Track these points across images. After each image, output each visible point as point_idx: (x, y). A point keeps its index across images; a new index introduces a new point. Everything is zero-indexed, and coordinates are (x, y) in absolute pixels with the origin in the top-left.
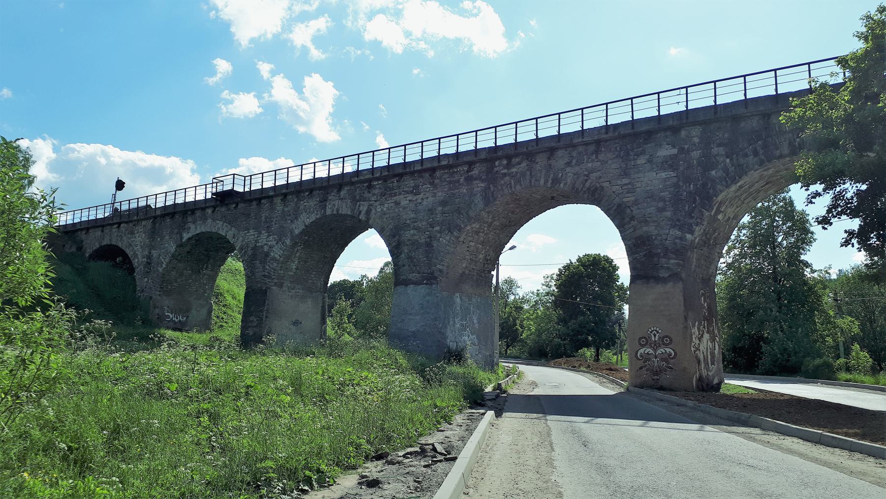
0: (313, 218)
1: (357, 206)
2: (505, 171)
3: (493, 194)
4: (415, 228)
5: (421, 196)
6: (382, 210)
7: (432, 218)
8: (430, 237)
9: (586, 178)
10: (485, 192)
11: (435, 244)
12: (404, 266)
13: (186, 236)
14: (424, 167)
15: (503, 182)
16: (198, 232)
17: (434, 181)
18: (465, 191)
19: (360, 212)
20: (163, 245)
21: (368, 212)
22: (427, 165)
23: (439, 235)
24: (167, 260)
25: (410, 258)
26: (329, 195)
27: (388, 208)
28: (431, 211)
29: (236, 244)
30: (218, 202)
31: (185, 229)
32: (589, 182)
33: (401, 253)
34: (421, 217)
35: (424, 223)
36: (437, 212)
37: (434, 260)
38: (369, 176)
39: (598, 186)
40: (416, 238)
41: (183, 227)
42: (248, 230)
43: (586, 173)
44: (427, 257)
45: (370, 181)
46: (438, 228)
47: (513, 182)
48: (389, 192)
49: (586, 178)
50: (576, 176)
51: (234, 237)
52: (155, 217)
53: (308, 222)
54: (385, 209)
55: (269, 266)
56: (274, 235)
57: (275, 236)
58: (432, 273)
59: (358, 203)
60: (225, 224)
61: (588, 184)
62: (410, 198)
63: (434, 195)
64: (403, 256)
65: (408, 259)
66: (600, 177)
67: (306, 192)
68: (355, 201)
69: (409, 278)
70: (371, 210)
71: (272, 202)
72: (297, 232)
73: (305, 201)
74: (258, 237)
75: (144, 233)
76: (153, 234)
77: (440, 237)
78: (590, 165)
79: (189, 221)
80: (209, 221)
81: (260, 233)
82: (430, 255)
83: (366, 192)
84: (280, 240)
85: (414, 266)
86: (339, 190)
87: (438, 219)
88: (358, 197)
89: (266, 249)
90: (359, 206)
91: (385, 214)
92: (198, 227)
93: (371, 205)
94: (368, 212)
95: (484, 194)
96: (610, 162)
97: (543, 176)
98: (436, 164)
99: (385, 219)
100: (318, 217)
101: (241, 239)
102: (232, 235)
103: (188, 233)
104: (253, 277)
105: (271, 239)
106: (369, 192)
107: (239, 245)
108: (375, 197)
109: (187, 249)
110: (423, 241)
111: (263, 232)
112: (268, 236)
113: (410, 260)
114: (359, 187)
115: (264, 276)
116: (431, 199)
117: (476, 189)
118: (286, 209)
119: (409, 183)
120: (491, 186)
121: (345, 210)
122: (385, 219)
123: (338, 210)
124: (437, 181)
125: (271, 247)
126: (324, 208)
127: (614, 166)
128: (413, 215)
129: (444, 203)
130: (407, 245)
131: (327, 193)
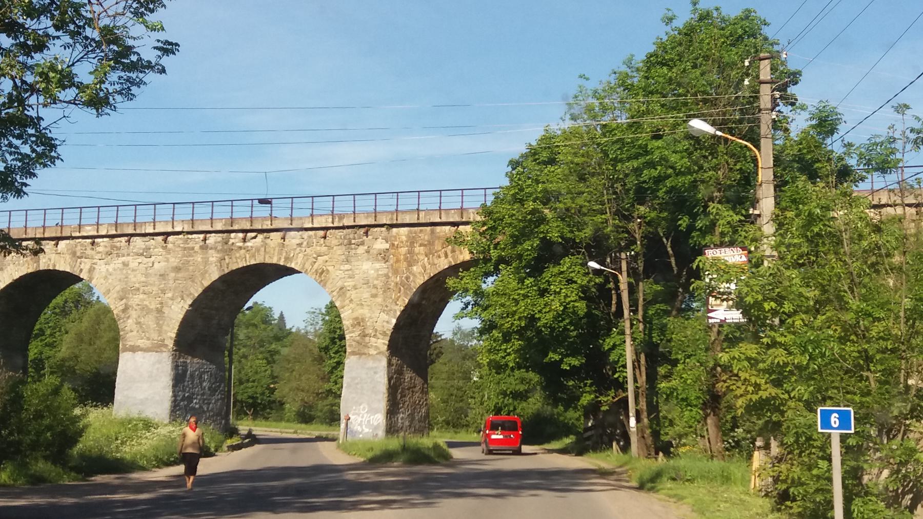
2: (241, 244)
3: (228, 264)
5: (153, 258)
11: (166, 310)
12: (132, 331)
18: (199, 259)
19: (81, 270)
23: (170, 302)
28: (163, 276)
34: (151, 282)
37: (165, 328)
40: (145, 303)
43: (315, 256)
44: (158, 324)
46: (170, 295)
47: (248, 256)
59: (79, 260)
61: (316, 266)
62: (140, 260)
63: (167, 260)
64: (130, 321)
69: (138, 344)
77: (173, 304)
78: (318, 248)
82: (161, 322)
88: (78, 254)
94: (91, 270)
96: (335, 248)
97: (276, 254)
108: (100, 255)
120: (226, 257)
123: (55, 266)
127: (339, 252)
128: (143, 279)
129: (177, 269)
130: (136, 310)
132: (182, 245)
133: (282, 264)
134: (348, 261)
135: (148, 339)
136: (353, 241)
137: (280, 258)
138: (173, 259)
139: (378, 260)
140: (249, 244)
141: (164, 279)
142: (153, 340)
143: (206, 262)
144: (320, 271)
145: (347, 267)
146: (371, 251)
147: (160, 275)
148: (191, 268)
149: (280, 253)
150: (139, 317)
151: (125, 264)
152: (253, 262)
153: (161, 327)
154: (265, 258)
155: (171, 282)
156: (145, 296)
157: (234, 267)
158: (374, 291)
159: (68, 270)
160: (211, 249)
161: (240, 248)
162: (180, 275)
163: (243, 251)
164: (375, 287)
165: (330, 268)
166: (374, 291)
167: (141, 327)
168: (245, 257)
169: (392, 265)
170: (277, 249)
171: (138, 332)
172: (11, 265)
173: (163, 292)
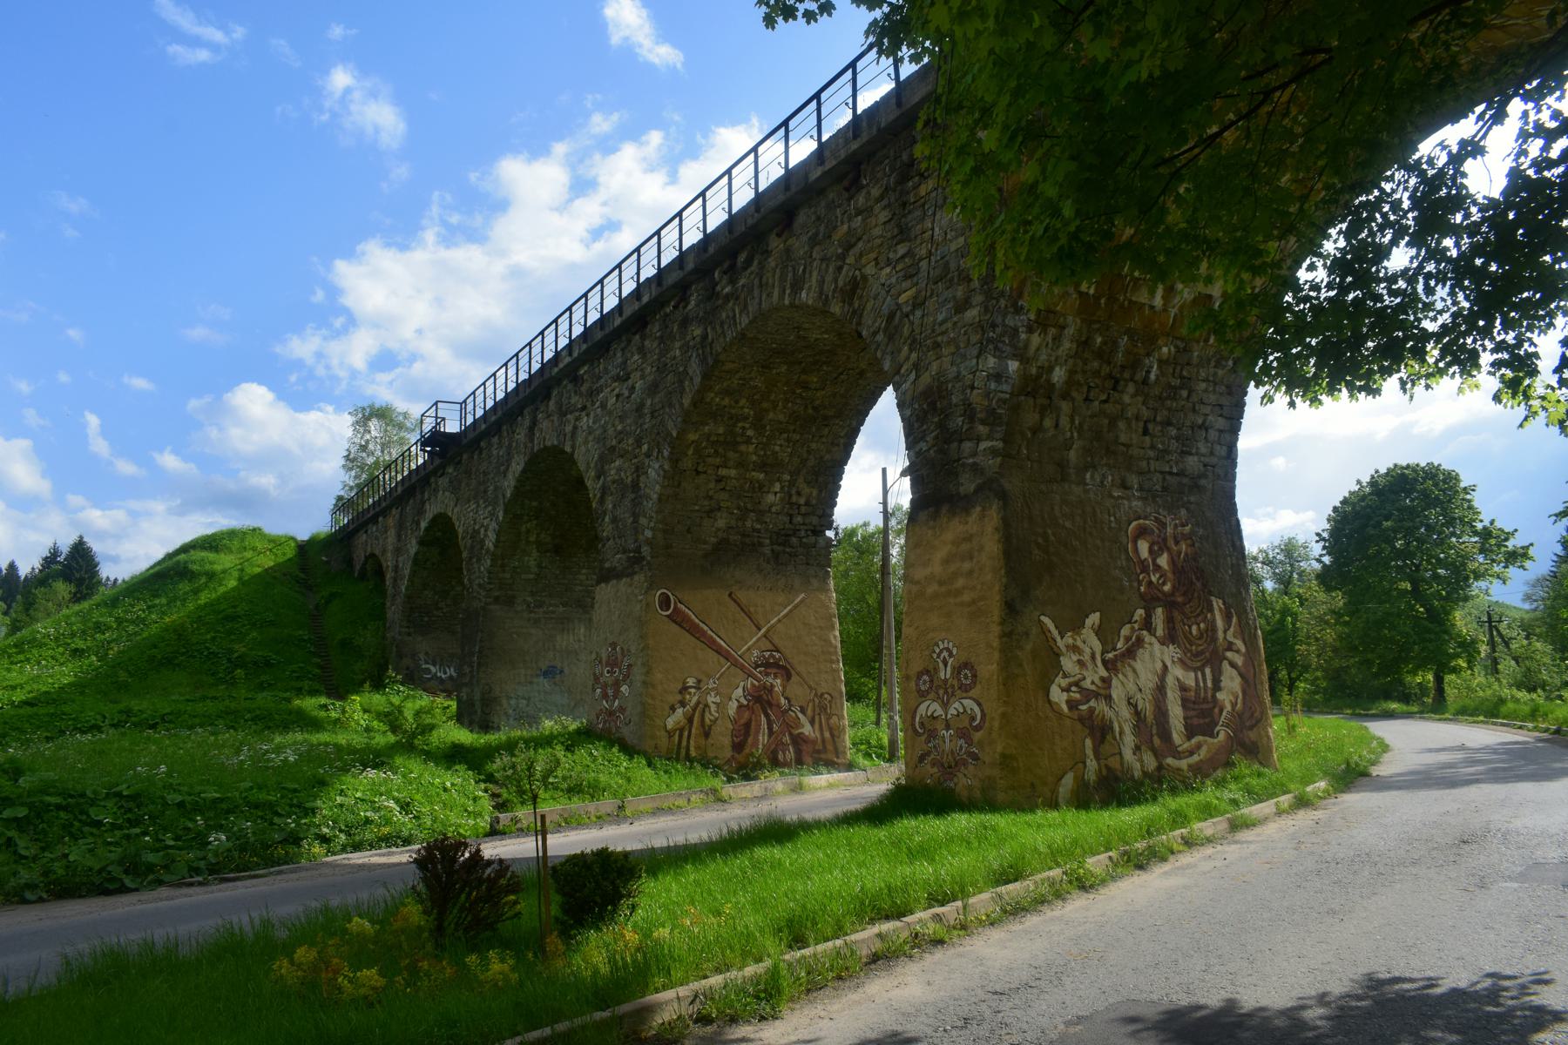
9: (840, 263)
15: (724, 315)
32: (846, 268)
61: (841, 283)
134: (903, 234)
144: (848, 288)
149: (783, 279)
161: (727, 298)
166: (960, 292)
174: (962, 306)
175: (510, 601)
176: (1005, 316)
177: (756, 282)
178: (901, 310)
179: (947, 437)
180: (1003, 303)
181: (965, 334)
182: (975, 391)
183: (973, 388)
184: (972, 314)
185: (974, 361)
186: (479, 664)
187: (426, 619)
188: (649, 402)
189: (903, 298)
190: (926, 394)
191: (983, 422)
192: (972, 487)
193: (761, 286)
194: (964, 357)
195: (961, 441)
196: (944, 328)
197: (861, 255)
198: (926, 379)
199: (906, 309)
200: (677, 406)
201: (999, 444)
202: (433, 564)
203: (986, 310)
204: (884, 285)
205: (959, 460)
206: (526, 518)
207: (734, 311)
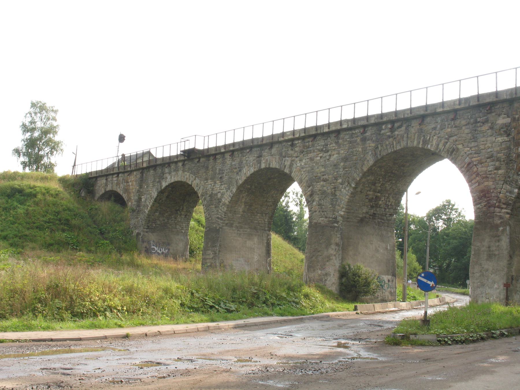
0: (252, 170)
1: (283, 161)
3: (380, 151)
4: (324, 180)
5: (329, 153)
6: (301, 165)
7: (337, 172)
8: (335, 188)
9: (446, 141)
10: (375, 151)
11: (338, 193)
12: (315, 212)
13: (164, 184)
14: (331, 129)
15: (387, 143)
16: (173, 181)
17: (338, 142)
18: (360, 149)
19: (285, 166)
20: (148, 192)
21: (291, 166)
22: (333, 128)
23: (341, 186)
24: (151, 204)
25: (320, 205)
26: (263, 152)
27: (305, 164)
28: (336, 166)
29: (198, 192)
30: (186, 158)
31: (163, 178)
32: (448, 143)
33: (313, 201)
35: (330, 176)
36: (340, 167)
37: (337, 207)
38: (291, 137)
39: (455, 148)
40: (325, 188)
41: (162, 177)
42: (207, 179)
43: (446, 137)
44: (332, 204)
45: (292, 140)
46: (340, 181)
47: (395, 143)
48: (306, 150)
49: (446, 141)
50: (439, 139)
51: (197, 186)
52: (143, 169)
53: (248, 174)
54: (303, 164)
55: (221, 210)
56: (225, 184)
57: (226, 186)
58: (336, 218)
59: (284, 159)
60: (191, 175)
61: (447, 146)
62: (320, 155)
63: (339, 154)
64: (314, 203)
65: (319, 205)
66: (456, 141)
67: (248, 149)
68: (282, 156)
69: (319, 221)
70: (293, 164)
71: (224, 157)
72: (240, 182)
73: (247, 157)
74: (213, 186)
75: (136, 181)
76: (142, 182)
77: (342, 188)
78: (449, 130)
79: (166, 172)
80: (180, 172)
81: (215, 183)
82: (334, 203)
83: (289, 149)
84: (229, 189)
85: (323, 212)
86: (271, 147)
87: (341, 173)
88: (284, 154)
89: (219, 195)
90: (285, 161)
91: (303, 168)
92: (173, 177)
93: (293, 161)
94: (291, 166)
95: (374, 153)
96: (464, 128)
98: (339, 127)
99: (303, 172)
100: (255, 170)
101: (202, 187)
102: (196, 184)
103: (166, 182)
104: (210, 219)
105: (223, 188)
106: (292, 150)
107: (201, 192)
108: (296, 153)
109: (166, 194)
110: (329, 191)
111: (217, 182)
112: (221, 185)
113: (320, 207)
114: (284, 145)
115: (218, 218)
116: (335, 156)
117: (368, 148)
118: (233, 163)
119: (320, 143)
120: (379, 146)
121: (274, 165)
122: (303, 172)
123: (270, 164)
124: (340, 141)
125: (223, 194)
126: (260, 163)
127: (467, 131)
128: (323, 170)
129: (345, 159)
130: (318, 195)
131: (263, 150)
132: (348, 140)
133: (420, 146)
135: (326, 218)
136: (479, 120)
137: (419, 143)
138: (342, 152)
139: (501, 135)
140: (396, 133)
141: (336, 168)
142: (329, 218)
143: (364, 150)
145: (473, 144)
146: (495, 127)
147: (335, 165)
148: (355, 157)
149: (419, 138)
150: (320, 200)
151: (311, 159)
152: (399, 148)
153: (335, 207)
154: (407, 143)
155: (341, 170)
156: (324, 183)
157: (384, 153)
158: (497, 164)
159: (277, 167)
160: (368, 140)
161: (389, 137)
162: (347, 164)
163: (391, 139)
164: (498, 160)
165: (460, 147)
167: (321, 208)
168: (393, 144)
169: (514, 138)
170: (416, 135)
171: (319, 212)
172: (246, 167)
173: (336, 179)
174: (497, 169)
175: (231, 225)
176: (513, 175)
177: (405, 135)
178: (473, 163)
179: (489, 206)
180: (513, 171)
181: (499, 177)
182: (501, 194)
183: (500, 193)
184: (500, 172)
185: (501, 186)
186: (219, 251)
187: (154, 225)
188: (342, 164)
189: (474, 159)
190: (482, 191)
191: (504, 204)
192: (499, 222)
193: (407, 137)
194: (498, 184)
195: (495, 207)
196: (490, 173)
197: (456, 141)
198: (482, 186)
199: (475, 163)
200: (360, 169)
201: (509, 211)
202: (162, 201)
203: (507, 171)
204: (466, 153)
205: (494, 213)
206: (244, 192)
207: (393, 143)
